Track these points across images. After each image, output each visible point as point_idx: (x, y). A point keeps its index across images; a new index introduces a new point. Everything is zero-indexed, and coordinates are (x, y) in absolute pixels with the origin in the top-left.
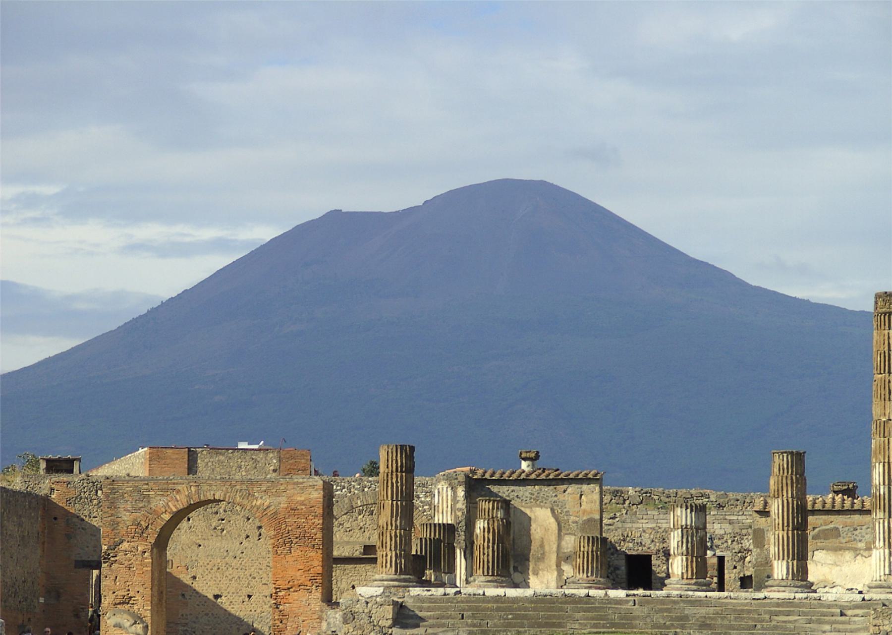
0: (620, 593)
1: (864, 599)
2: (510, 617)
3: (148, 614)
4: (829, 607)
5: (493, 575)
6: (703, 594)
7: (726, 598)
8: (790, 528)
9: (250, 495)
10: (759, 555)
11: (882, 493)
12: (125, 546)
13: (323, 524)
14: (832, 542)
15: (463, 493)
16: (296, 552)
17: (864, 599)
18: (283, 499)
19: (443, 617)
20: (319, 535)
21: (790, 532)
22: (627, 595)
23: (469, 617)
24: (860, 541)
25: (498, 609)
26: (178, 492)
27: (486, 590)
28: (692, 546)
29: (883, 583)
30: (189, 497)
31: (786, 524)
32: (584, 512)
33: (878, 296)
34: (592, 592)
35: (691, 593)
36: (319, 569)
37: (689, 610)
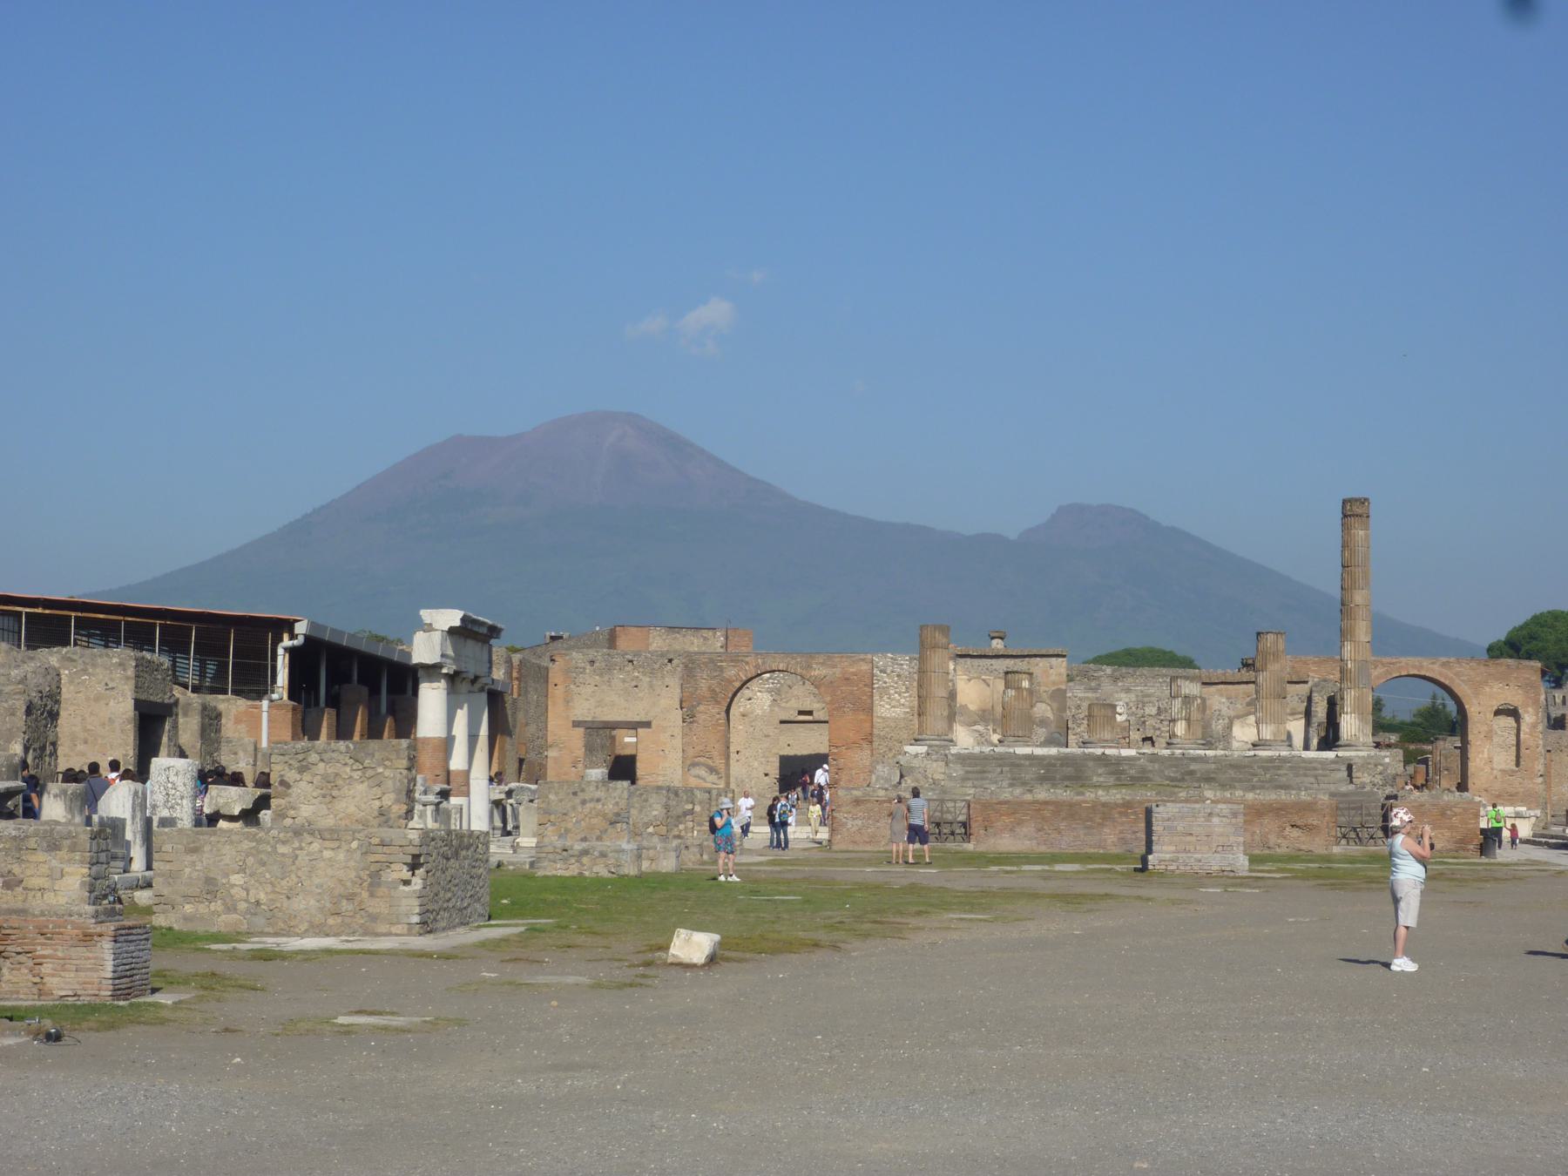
6: (1201, 752)
12: (701, 708)
18: (838, 671)
30: (757, 667)
32: (1054, 683)
33: (1345, 502)
34: (1108, 752)
37: (1193, 767)
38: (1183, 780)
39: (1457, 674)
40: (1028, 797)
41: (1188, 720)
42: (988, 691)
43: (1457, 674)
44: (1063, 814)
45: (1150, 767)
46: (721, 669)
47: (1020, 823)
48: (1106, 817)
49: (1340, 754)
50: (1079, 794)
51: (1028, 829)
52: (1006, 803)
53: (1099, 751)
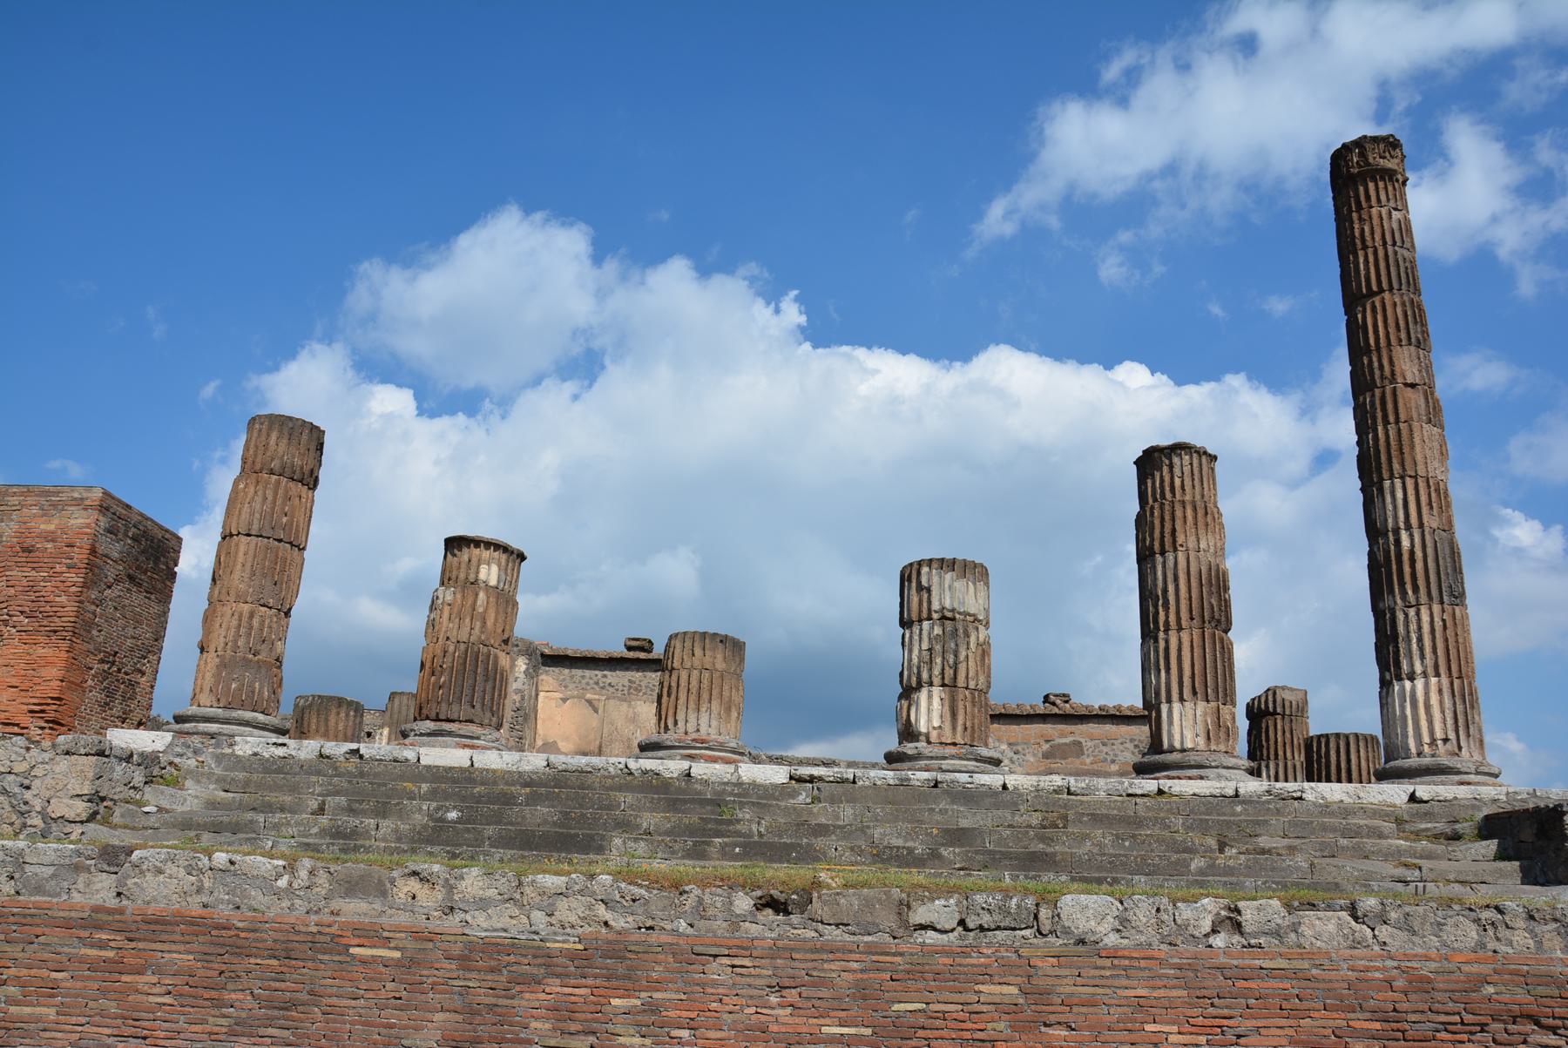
1: (1413, 798)
2: (453, 815)
13: (85, 585)
14: (1074, 763)
15: (524, 667)
17: (1413, 798)
20: (71, 608)
22: (791, 778)
23: (339, 809)
24: (1113, 761)
25: (432, 795)
27: (423, 751)
34: (700, 769)
35: (963, 778)
38: (934, 855)
40: (100, 889)
41: (950, 685)
42: (594, 721)
44: (241, 1001)
45: (822, 814)
49: (1423, 791)
50: (352, 887)
53: (672, 767)
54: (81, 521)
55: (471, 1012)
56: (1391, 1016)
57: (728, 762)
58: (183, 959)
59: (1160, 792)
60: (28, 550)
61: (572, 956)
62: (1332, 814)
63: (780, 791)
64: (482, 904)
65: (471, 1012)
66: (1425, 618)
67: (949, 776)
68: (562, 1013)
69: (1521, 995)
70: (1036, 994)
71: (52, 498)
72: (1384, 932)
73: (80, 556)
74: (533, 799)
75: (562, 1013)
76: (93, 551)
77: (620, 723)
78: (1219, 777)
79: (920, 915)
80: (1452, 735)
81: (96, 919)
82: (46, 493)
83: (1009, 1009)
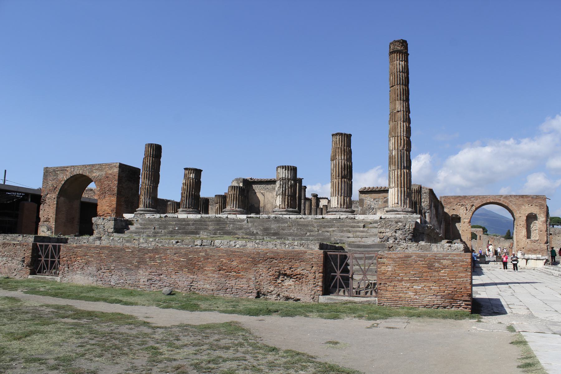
0: (244, 217)
1: (381, 218)
3: (54, 226)
4: (358, 222)
5: (186, 208)
6: (287, 216)
7: (301, 218)
8: (340, 177)
9: (92, 171)
10: (361, 210)
11: (394, 154)
16: (107, 198)
19: (146, 228)
20: (116, 189)
21: (340, 180)
26: (67, 171)
28: (285, 190)
29: (394, 209)
31: (337, 175)
34: (229, 216)
35: (281, 216)
36: (115, 206)
39: (510, 201)
40: (98, 243)
43: (510, 201)
46: (56, 175)
47: (87, 263)
48: (141, 262)
51: (92, 269)
52: (81, 247)
54: (116, 170)
55: (140, 258)
56: (253, 258)
57: (235, 214)
58: (107, 252)
59: (323, 218)
60: (107, 177)
61: (151, 250)
62: (355, 223)
63: (243, 220)
64: (143, 243)
65: (140, 258)
66: (396, 173)
67: (278, 216)
68: (150, 257)
69: (272, 255)
70: (207, 255)
71: (110, 166)
72: (259, 246)
73: (117, 178)
74: (193, 224)
75: (150, 257)
76: (119, 176)
77: (270, 198)
78: (339, 214)
79: (196, 244)
80: (399, 202)
81: (97, 247)
82: (109, 165)
83: (204, 257)
